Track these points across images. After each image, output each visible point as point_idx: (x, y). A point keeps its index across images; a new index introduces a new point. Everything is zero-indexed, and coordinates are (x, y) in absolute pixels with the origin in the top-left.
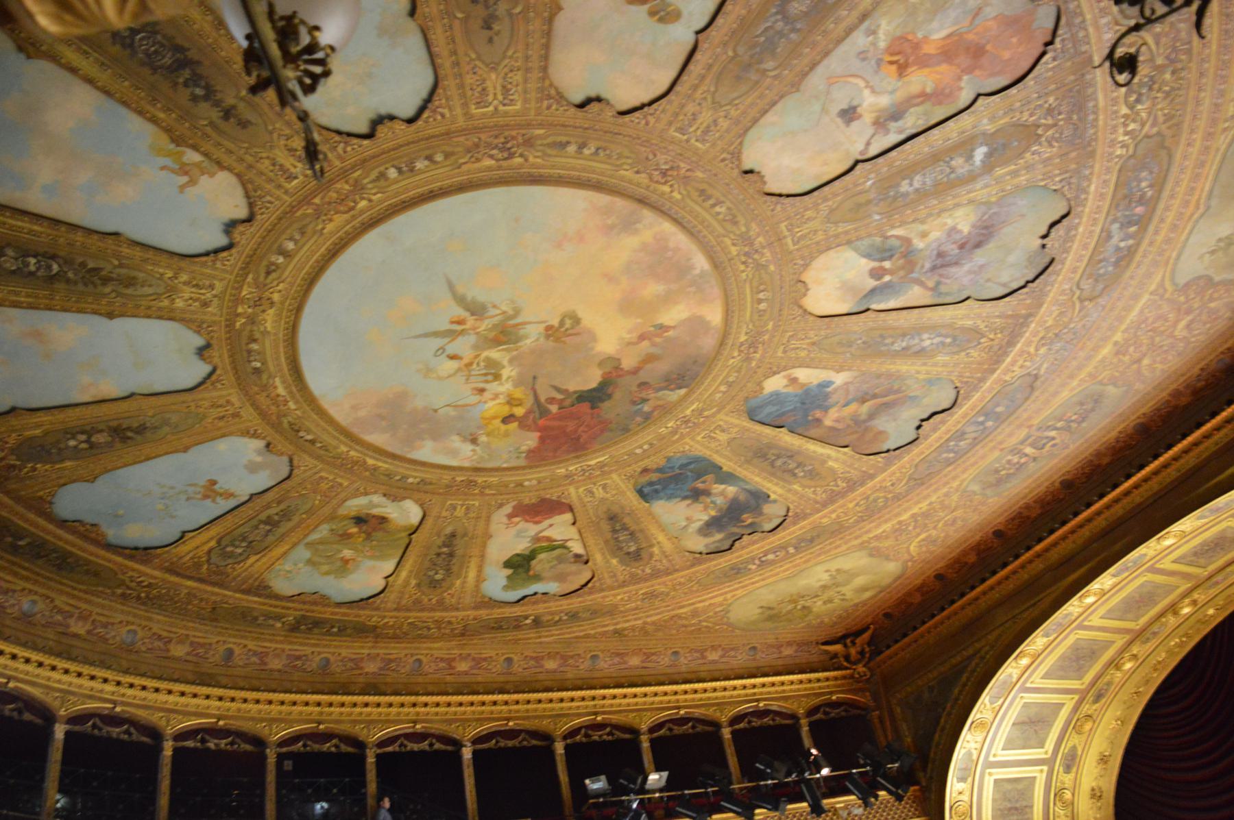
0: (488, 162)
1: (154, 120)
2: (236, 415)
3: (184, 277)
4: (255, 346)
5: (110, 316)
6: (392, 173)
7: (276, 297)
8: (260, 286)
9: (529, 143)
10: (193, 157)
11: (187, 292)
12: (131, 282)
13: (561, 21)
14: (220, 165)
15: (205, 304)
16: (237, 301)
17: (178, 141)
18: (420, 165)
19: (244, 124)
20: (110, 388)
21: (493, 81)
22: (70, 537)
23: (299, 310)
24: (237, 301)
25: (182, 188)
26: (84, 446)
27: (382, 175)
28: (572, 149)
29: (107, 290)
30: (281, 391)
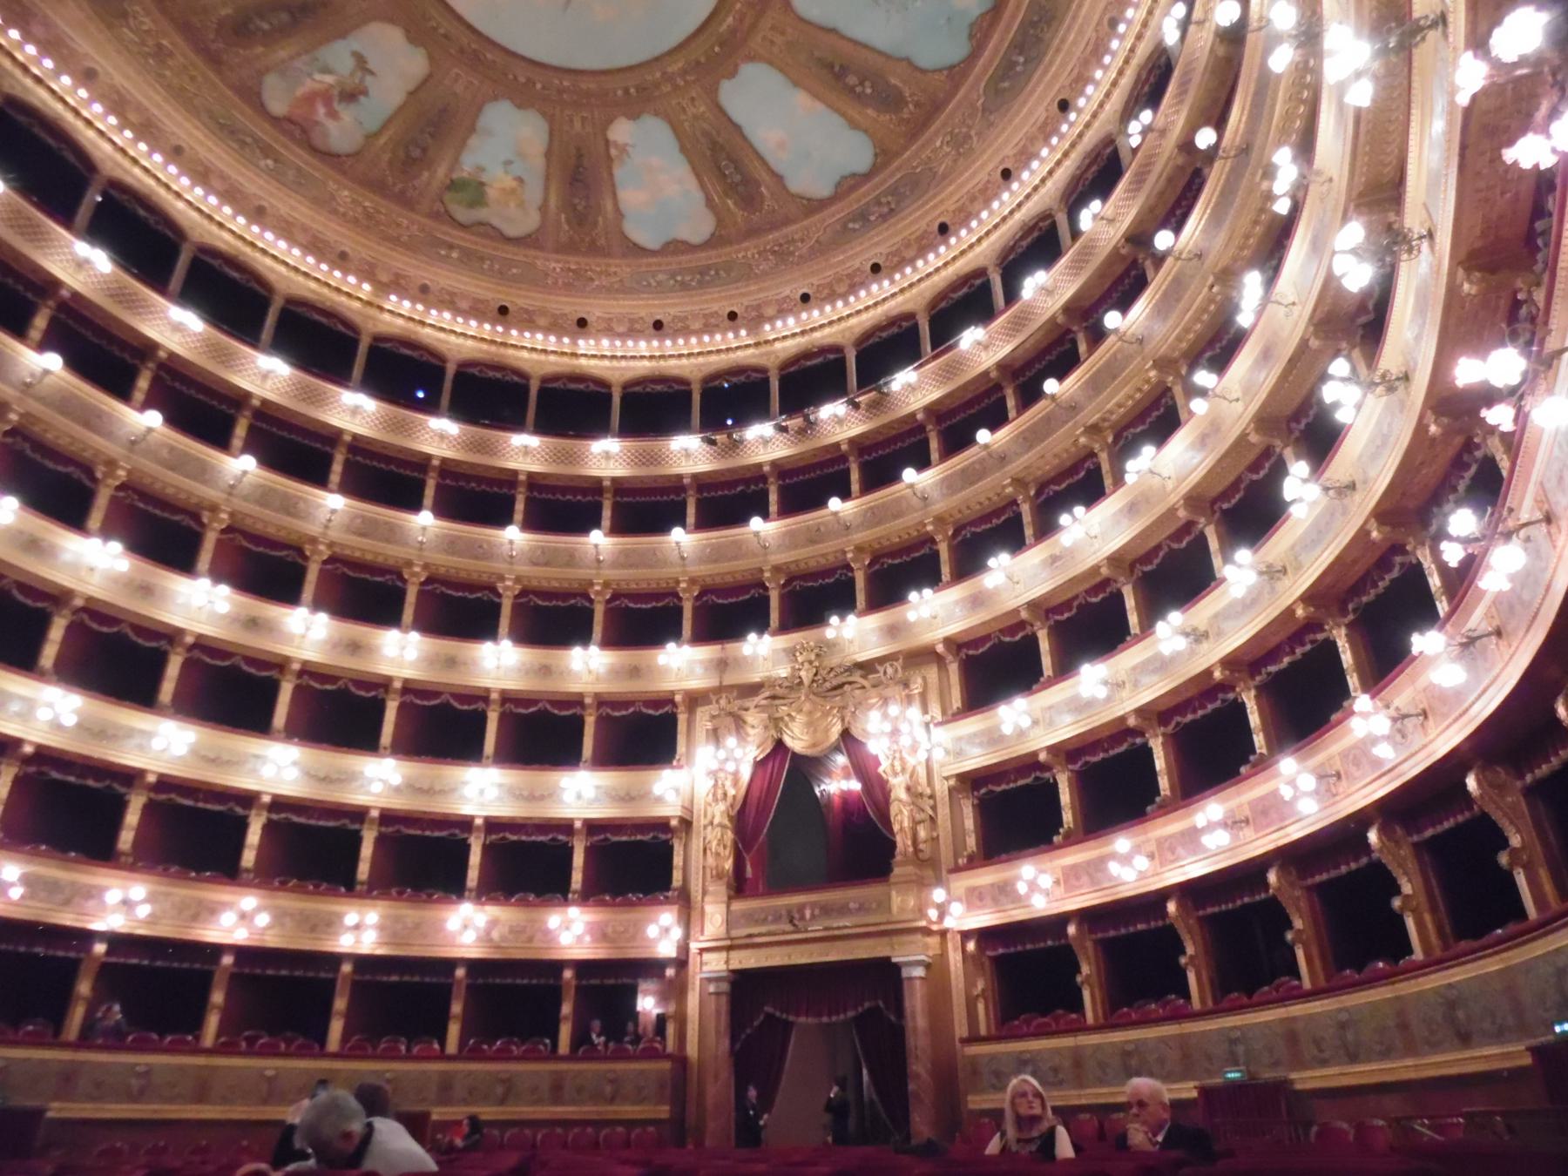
0: (489, 56)
1: (611, 175)
2: (773, 28)
3: (683, 117)
4: (703, 60)
5: (737, 128)
6: (539, 86)
7: (658, 75)
8: (657, 85)
9: (462, 51)
10: (613, 152)
11: (691, 111)
12: (706, 134)
13: (411, 87)
14: (607, 142)
15: (693, 99)
16: (676, 87)
17: (609, 159)
18: (522, 80)
19: (578, 149)
20: (801, 99)
21: (459, 88)
22: (996, 37)
23: (657, 59)
24: (676, 87)
25: (633, 146)
26: (867, 84)
27: (544, 88)
28: (442, 31)
29: (720, 140)
30: (730, 20)
